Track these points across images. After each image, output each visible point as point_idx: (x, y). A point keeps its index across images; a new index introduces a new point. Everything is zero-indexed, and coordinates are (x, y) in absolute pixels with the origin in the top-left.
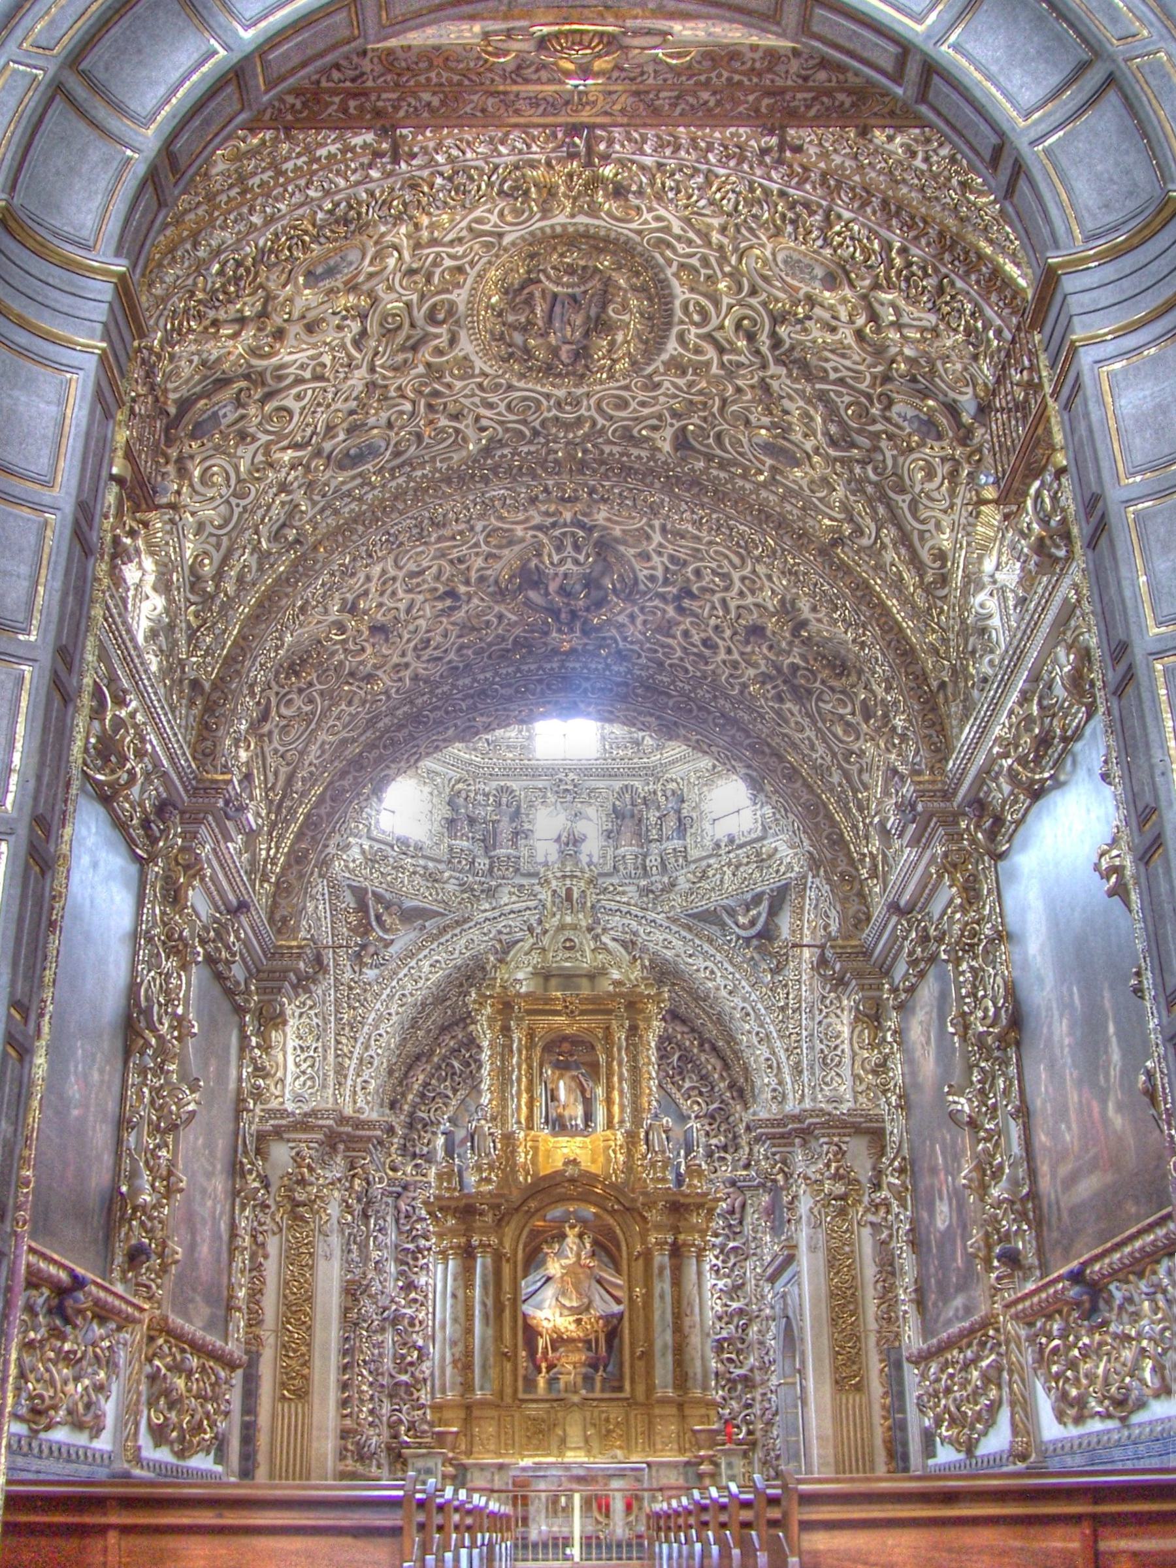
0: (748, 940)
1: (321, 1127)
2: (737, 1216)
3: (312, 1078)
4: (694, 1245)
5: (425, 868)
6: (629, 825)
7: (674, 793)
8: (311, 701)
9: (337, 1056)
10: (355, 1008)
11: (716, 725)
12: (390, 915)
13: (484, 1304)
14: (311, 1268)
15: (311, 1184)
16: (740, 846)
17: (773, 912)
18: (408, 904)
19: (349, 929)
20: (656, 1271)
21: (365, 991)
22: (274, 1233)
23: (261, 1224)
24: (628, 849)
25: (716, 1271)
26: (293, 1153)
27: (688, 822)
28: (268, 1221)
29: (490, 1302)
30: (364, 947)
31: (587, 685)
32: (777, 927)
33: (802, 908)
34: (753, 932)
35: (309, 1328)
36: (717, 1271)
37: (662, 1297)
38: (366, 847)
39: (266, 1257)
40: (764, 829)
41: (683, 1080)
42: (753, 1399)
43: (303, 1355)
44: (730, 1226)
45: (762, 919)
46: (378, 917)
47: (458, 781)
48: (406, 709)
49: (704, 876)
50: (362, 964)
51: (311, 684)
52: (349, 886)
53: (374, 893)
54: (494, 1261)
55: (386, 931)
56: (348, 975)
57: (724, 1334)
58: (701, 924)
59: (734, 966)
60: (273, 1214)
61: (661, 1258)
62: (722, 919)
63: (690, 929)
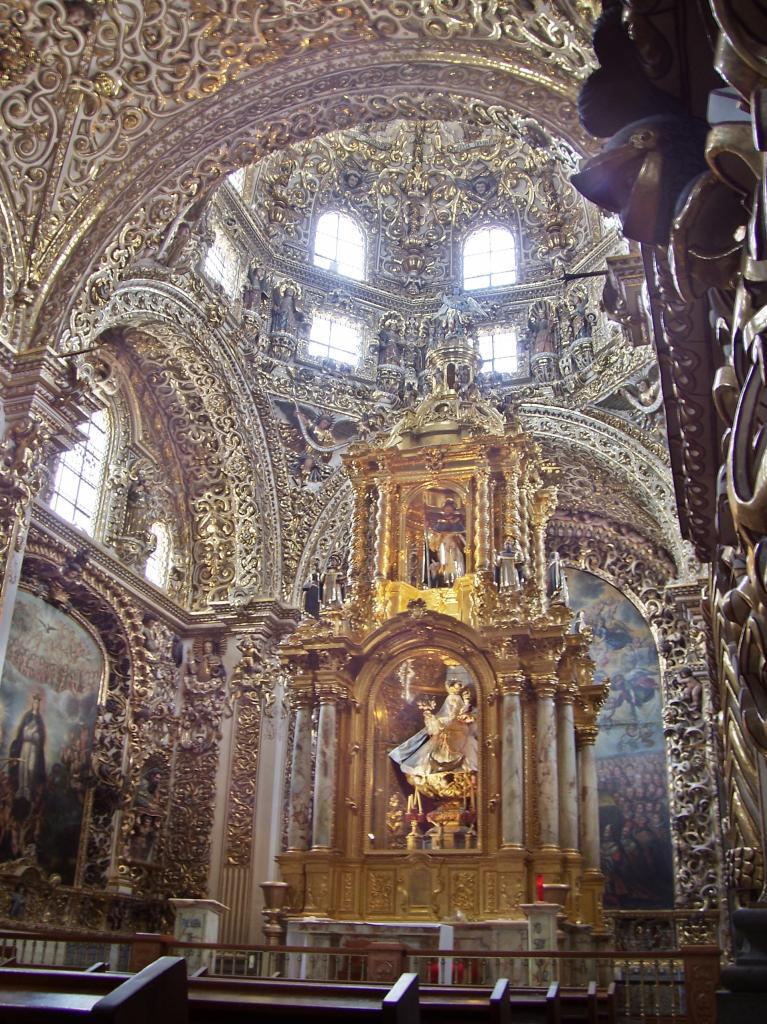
0: (652, 415)
1: (261, 619)
2: (695, 703)
3: (256, 576)
4: (548, 685)
5: (354, 387)
6: (543, 333)
7: (580, 300)
8: (45, 111)
10: (300, 517)
11: (488, 84)
12: (322, 429)
13: (324, 754)
14: (255, 746)
15: (258, 672)
18: (338, 419)
20: (504, 714)
21: (310, 501)
22: (228, 717)
23: (216, 709)
24: (541, 356)
25: (676, 753)
26: (239, 643)
27: (591, 318)
28: (223, 706)
29: (331, 752)
30: (302, 461)
31: (356, 77)
34: (655, 406)
35: (252, 801)
36: (678, 756)
37: (510, 741)
39: (219, 738)
41: (641, 585)
42: (715, 874)
43: (247, 825)
44: (689, 714)
46: (310, 432)
47: (390, 317)
48: (177, 134)
49: (607, 364)
51: (35, 89)
53: (301, 408)
54: (338, 712)
55: (320, 444)
56: (290, 486)
57: (684, 812)
58: (612, 412)
59: (647, 448)
60: (227, 700)
61: (513, 700)
62: (628, 402)
63: (603, 419)
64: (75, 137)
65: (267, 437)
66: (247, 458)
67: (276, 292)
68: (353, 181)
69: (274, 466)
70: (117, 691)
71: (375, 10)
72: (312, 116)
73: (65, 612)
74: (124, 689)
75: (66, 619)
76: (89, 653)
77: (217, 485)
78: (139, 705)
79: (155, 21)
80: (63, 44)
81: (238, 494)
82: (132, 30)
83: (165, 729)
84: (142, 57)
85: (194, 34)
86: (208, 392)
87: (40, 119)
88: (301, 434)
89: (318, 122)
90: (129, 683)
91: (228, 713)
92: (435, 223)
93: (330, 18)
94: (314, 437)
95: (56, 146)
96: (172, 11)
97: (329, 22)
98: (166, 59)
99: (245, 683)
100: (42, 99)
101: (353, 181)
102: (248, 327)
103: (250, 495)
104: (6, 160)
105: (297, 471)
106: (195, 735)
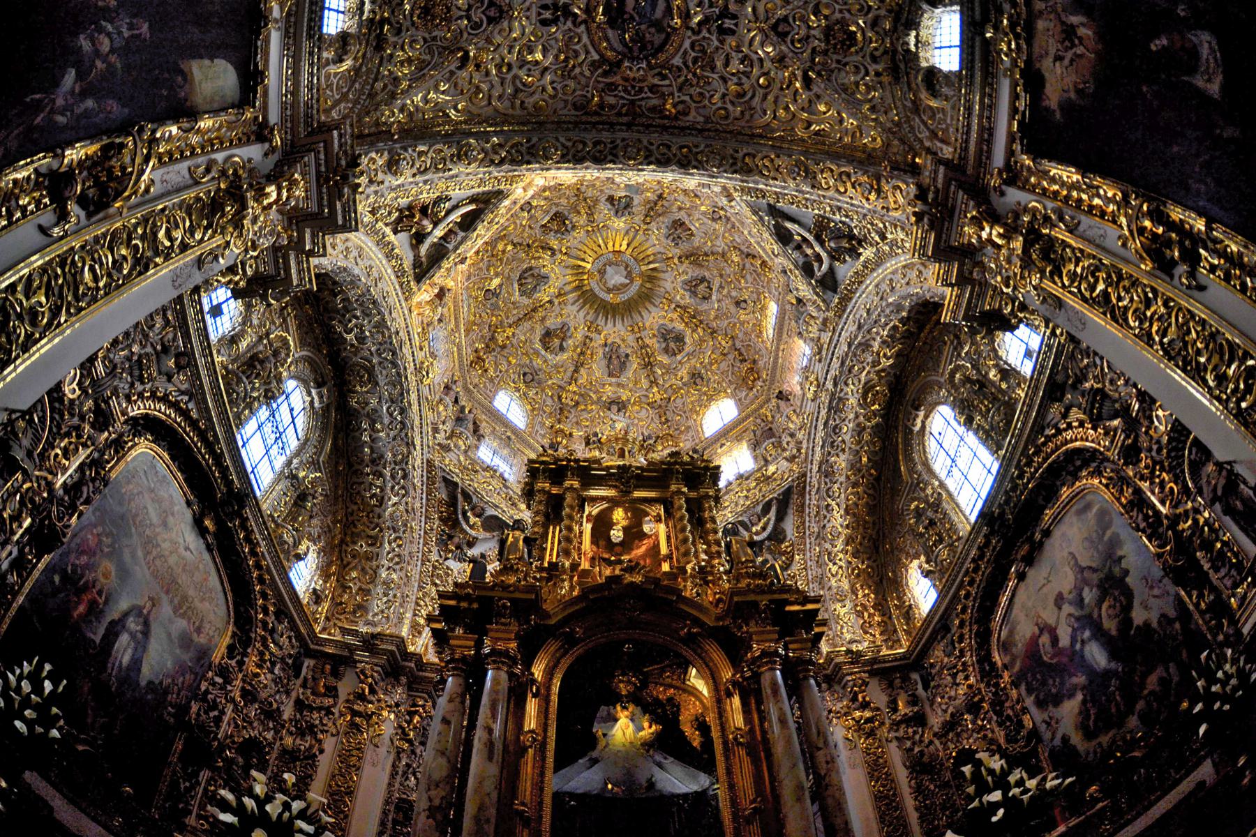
5: (507, 494)
9: (415, 615)
16: (747, 479)
17: (780, 517)
18: (490, 512)
19: (440, 519)
30: (450, 537)
32: (784, 531)
33: (803, 505)
34: (765, 534)
38: (462, 458)
39: (322, 751)
40: (766, 461)
45: (772, 522)
46: (464, 513)
50: (448, 551)
52: (445, 479)
55: (471, 527)
56: (434, 557)
65: (427, 505)
66: (407, 511)
67: (463, 408)
68: (529, 377)
69: (425, 532)
70: (233, 663)
73: (209, 548)
74: (241, 664)
75: (207, 556)
76: (217, 606)
77: (370, 537)
78: (250, 684)
81: (390, 543)
83: (271, 725)
86: (394, 439)
88: (455, 512)
90: (246, 659)
91: (334, 731)
92: (577, 423)
94: (467, 519)
97: (643, 95)
99: (356, 707)
101: (529, 377)
102: (441, 408)
103: (399, 546)
105: (443, 543)
106: (298, 741)
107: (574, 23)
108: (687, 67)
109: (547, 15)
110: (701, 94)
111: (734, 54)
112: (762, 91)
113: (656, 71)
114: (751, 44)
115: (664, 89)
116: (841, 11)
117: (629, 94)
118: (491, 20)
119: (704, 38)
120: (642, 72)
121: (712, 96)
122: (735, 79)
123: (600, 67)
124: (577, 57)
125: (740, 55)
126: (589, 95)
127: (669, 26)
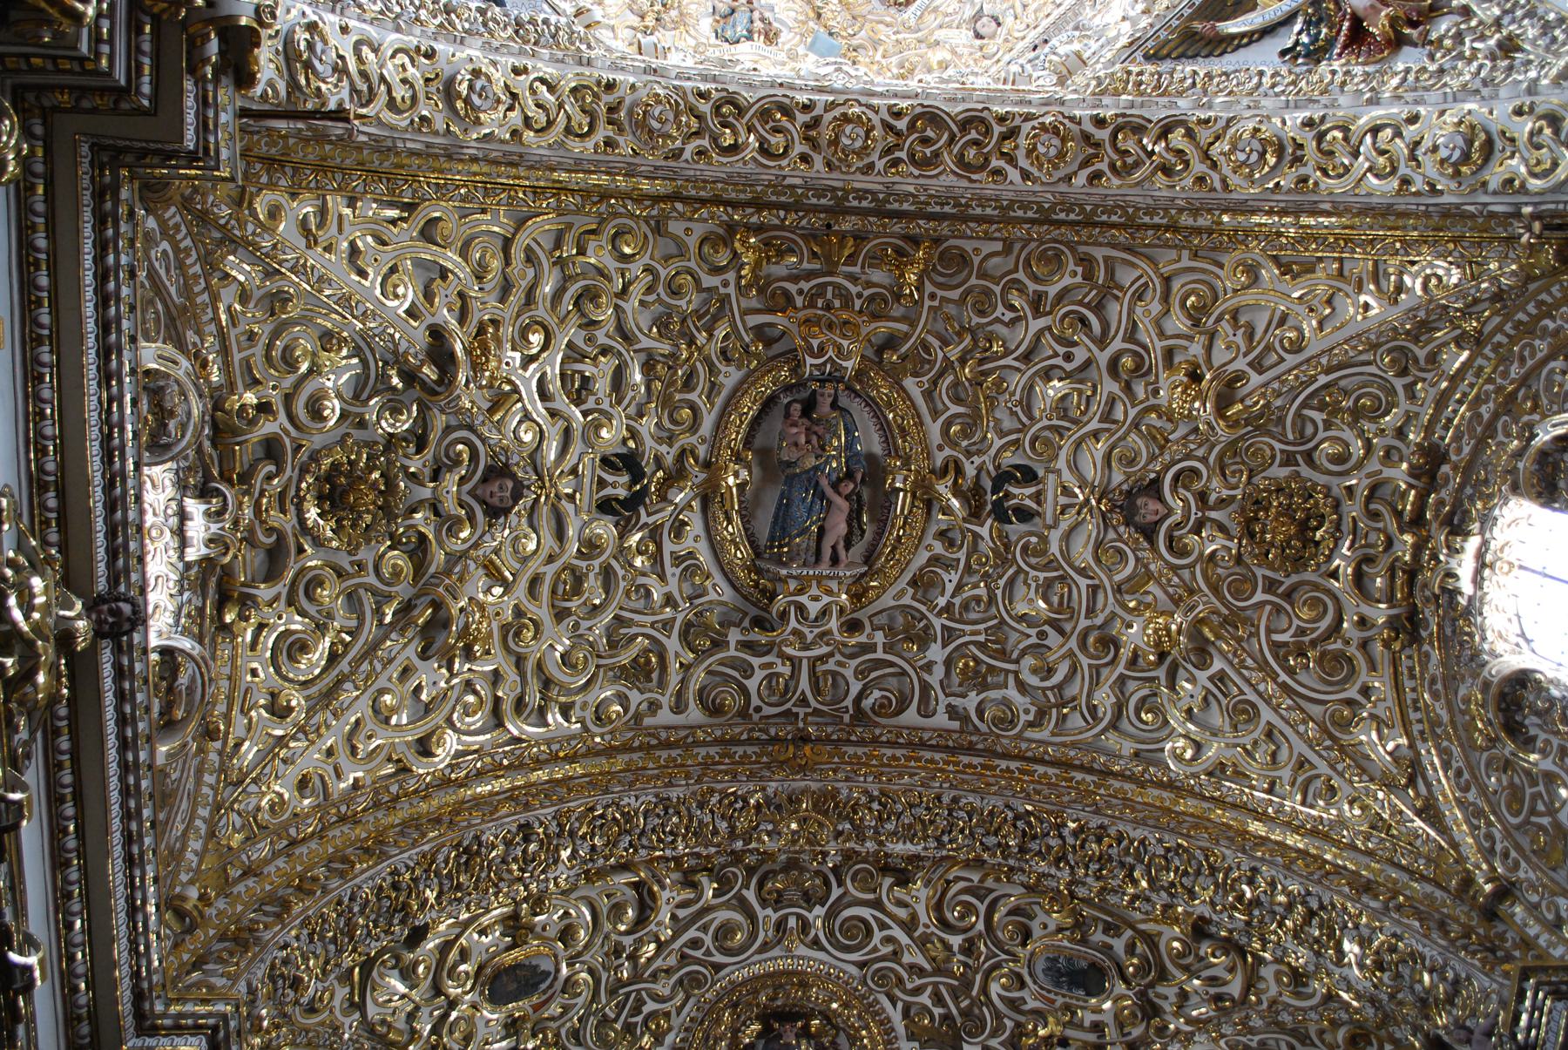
64: (1291, 360)
71: (722, 290)
72: (903, 155)
79: (1055, 422)
80: (1198, 486)
82: (1096, 435)
84: (1110, 386)
85: (1016, 364)
87: (1319, 417)
89: (898, 134)
93: (800, 292)
95: (1328, 372)
96: (1024, 419)
97: (805, 286)
98: (1080, 355)
100: (1291, 437)
104: (1417, 414)
107: (959, 471)
108: (708, 361)
109: (1021, 494)
110: (675, 293)
111: (605, 406)
112: (541, 312)
113: (777, 348)
114: (567, 433)
115: (755, 304)
116: (361, 566)
117: (837, 286)
118: (1153, 488)
119: (670, 440)
120: (815, 343)
121: (650, 289)
122: (602, 339)
123: (903, 358)
124: (956, 384)
125: (590, 404)
126: (929, 288)
127: (749, 467)
